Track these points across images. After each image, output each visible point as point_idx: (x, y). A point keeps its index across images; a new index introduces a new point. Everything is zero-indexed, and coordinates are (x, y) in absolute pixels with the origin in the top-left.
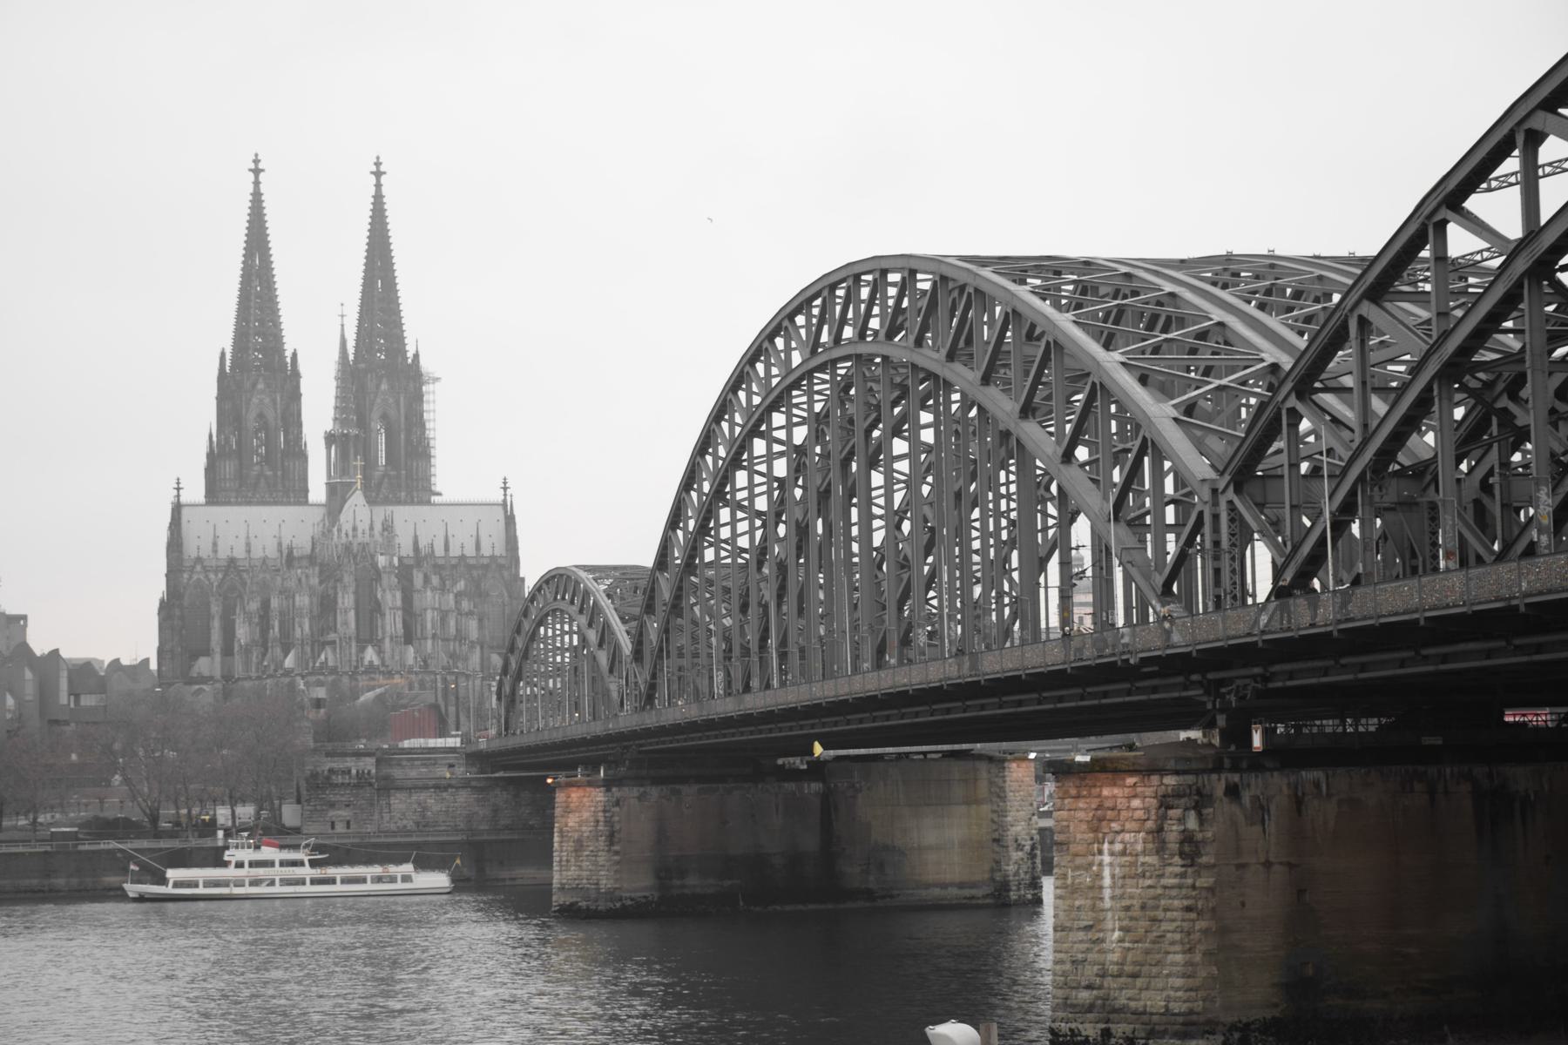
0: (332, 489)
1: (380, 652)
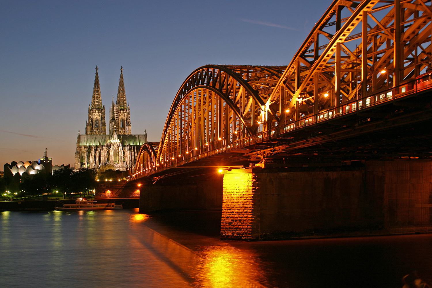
0: (110, 132)
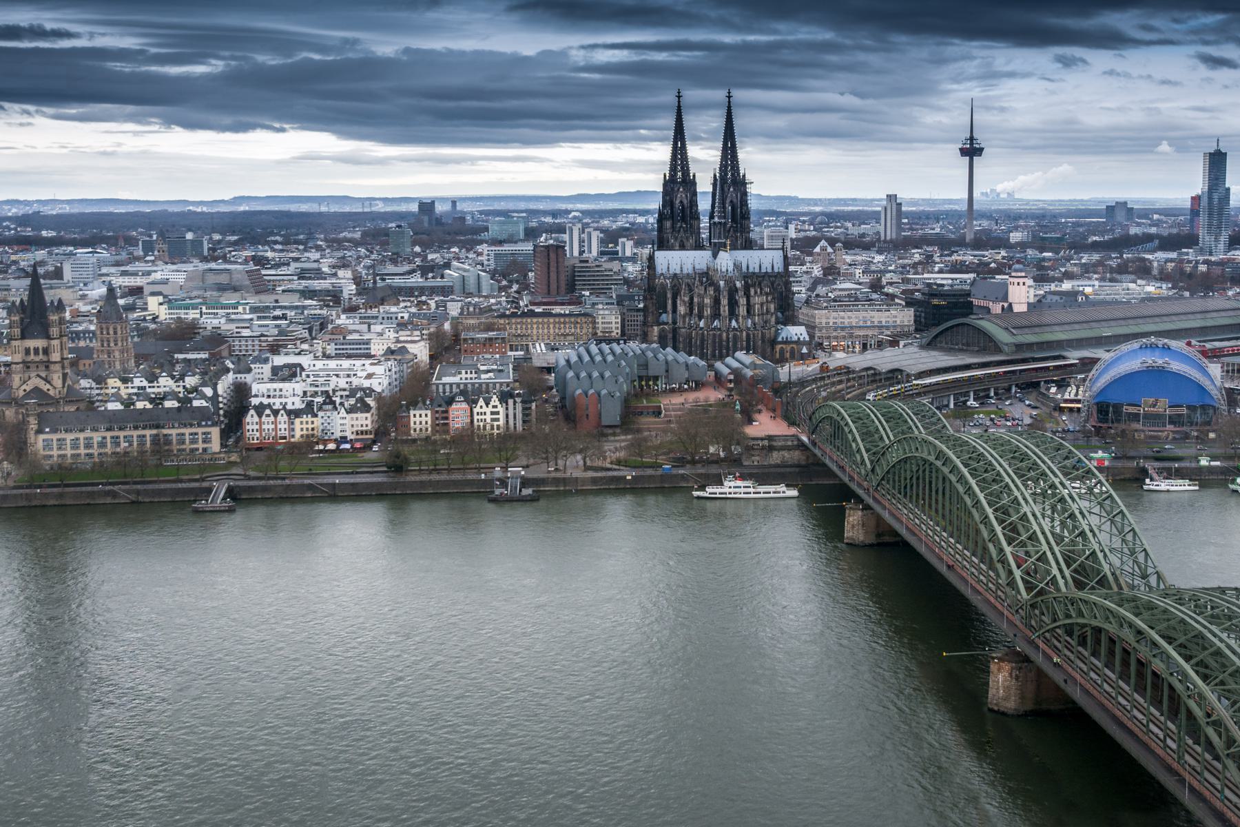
1: (737, 321)
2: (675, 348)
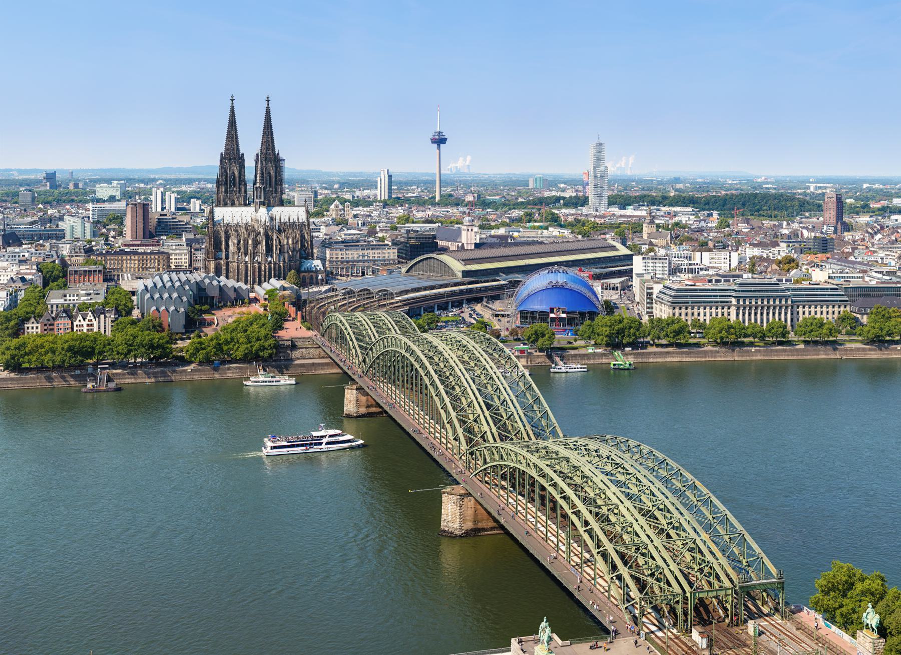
2: (227, 277)
